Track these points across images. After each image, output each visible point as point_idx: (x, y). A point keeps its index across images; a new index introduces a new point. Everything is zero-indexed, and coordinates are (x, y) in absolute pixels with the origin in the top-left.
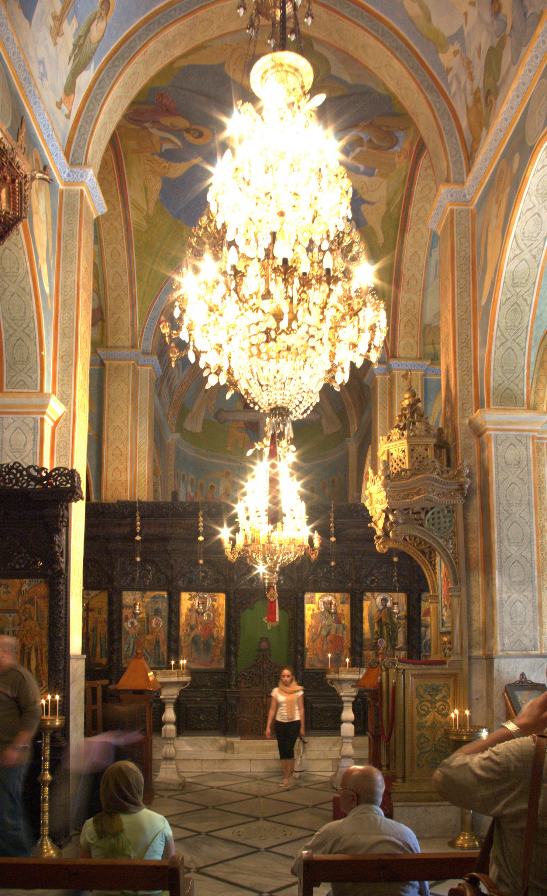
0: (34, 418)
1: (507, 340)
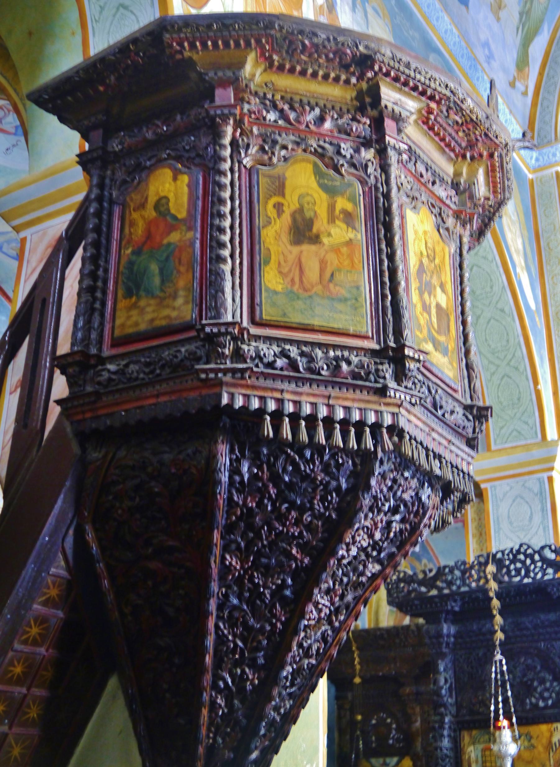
0: (539, 479)
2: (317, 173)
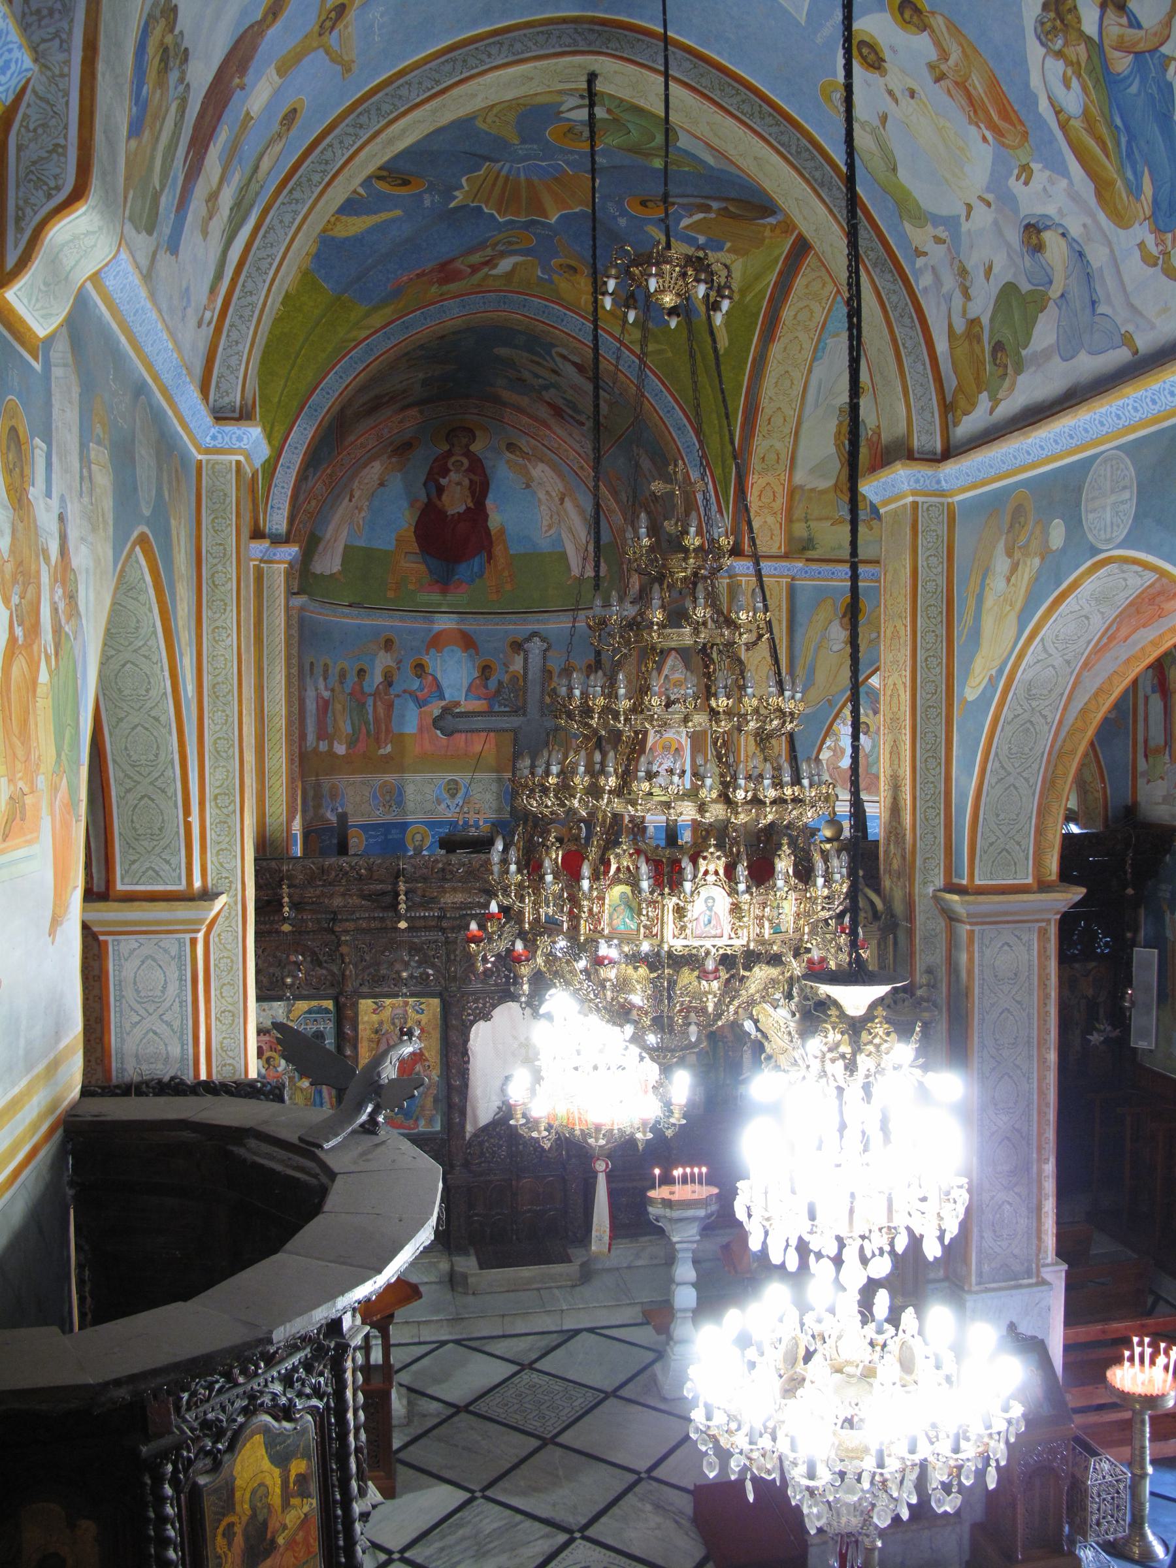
0: (178, 940)
1: (1009, 774)
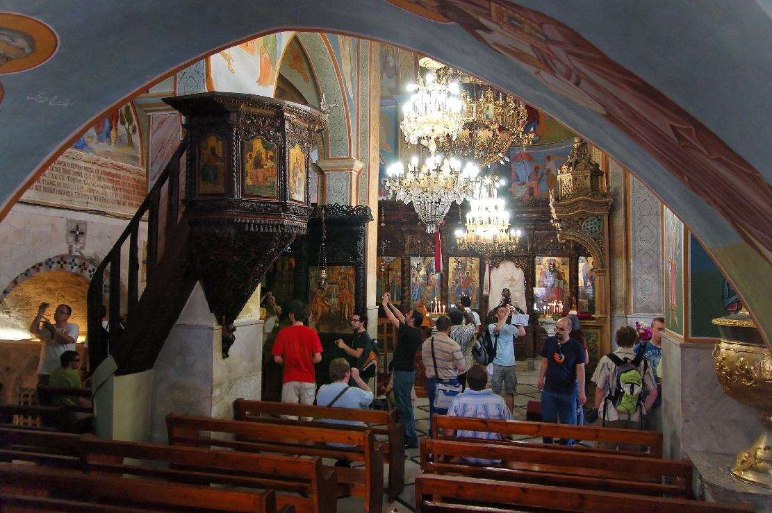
2: (263, 143)
